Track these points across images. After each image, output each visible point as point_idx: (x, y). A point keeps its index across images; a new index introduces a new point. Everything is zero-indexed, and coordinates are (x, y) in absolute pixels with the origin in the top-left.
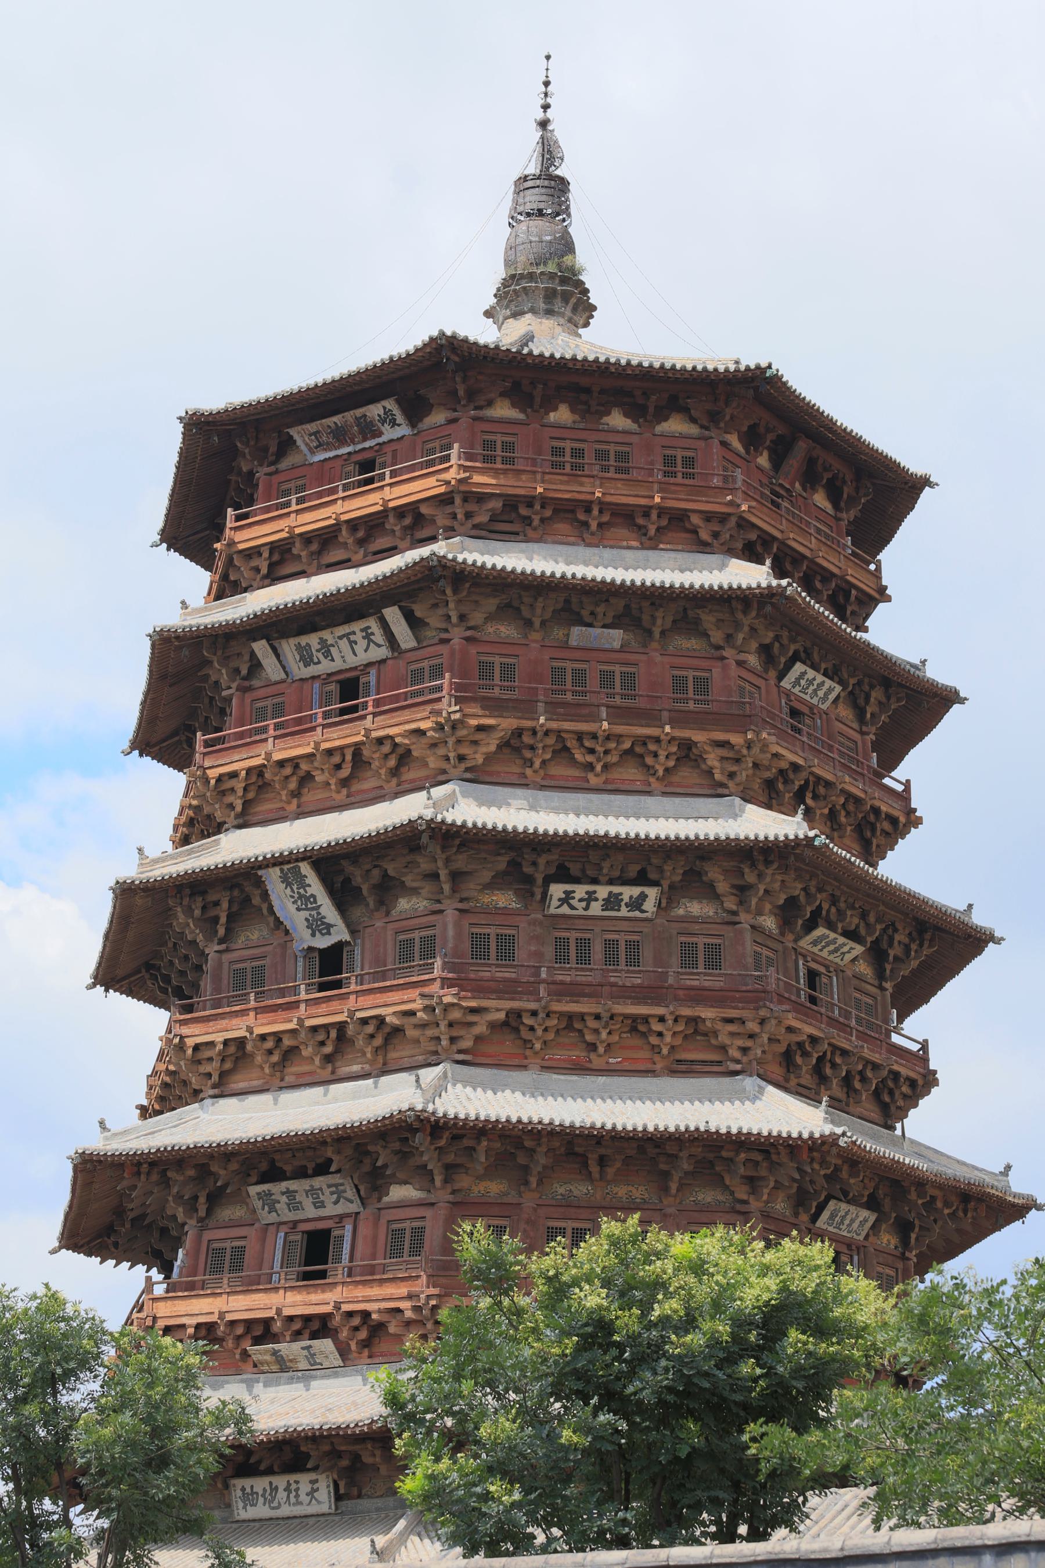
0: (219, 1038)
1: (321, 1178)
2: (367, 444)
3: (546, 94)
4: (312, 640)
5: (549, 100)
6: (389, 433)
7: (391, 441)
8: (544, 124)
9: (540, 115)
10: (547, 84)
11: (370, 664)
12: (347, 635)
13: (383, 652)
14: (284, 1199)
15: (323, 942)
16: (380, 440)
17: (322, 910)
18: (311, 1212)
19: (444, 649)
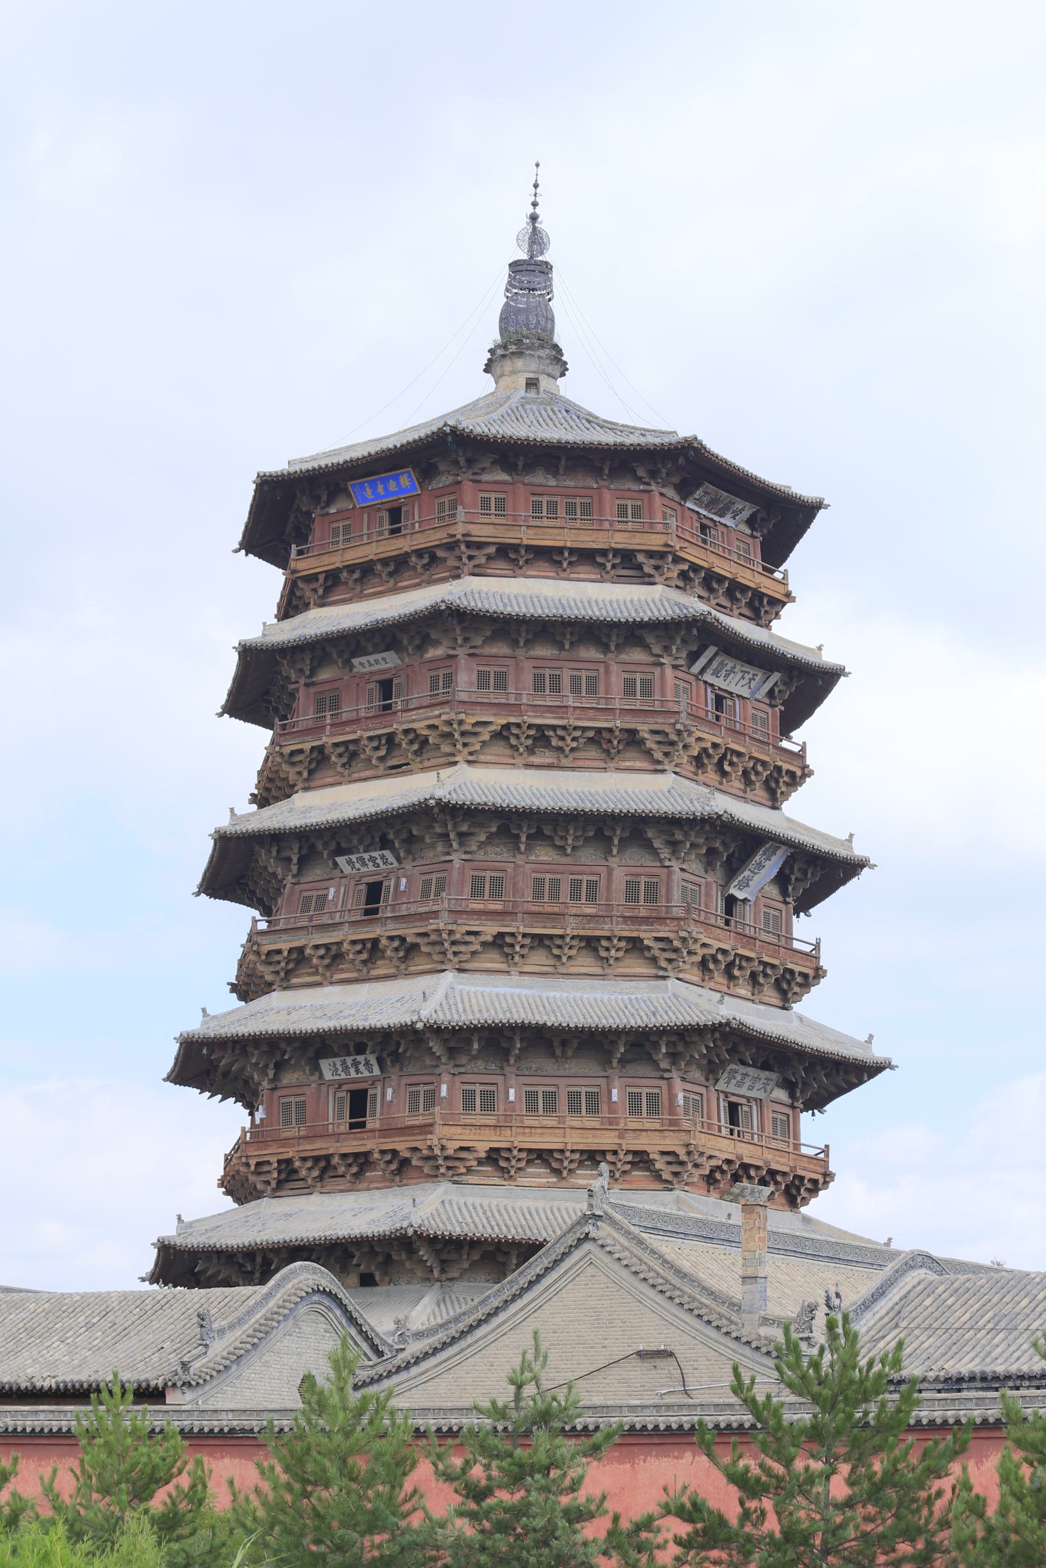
0: (717, 945)
1: (767, 1073)
2: (715, 518)
3: (535, 195)
4: (730, 664)
5: (538, 199)
6: (727, 520)
7: (725, 525)
8: (534, 218)
9: (530, 210)
10: (536, 186)
11: (738, 696)
12: (745, 672)
13: (745, 692)
14: (739, 1078)
15: (740, 895)
16: (722, 520)
17: (756, 877)
18: (743, 1091)
19: (769, 710)
